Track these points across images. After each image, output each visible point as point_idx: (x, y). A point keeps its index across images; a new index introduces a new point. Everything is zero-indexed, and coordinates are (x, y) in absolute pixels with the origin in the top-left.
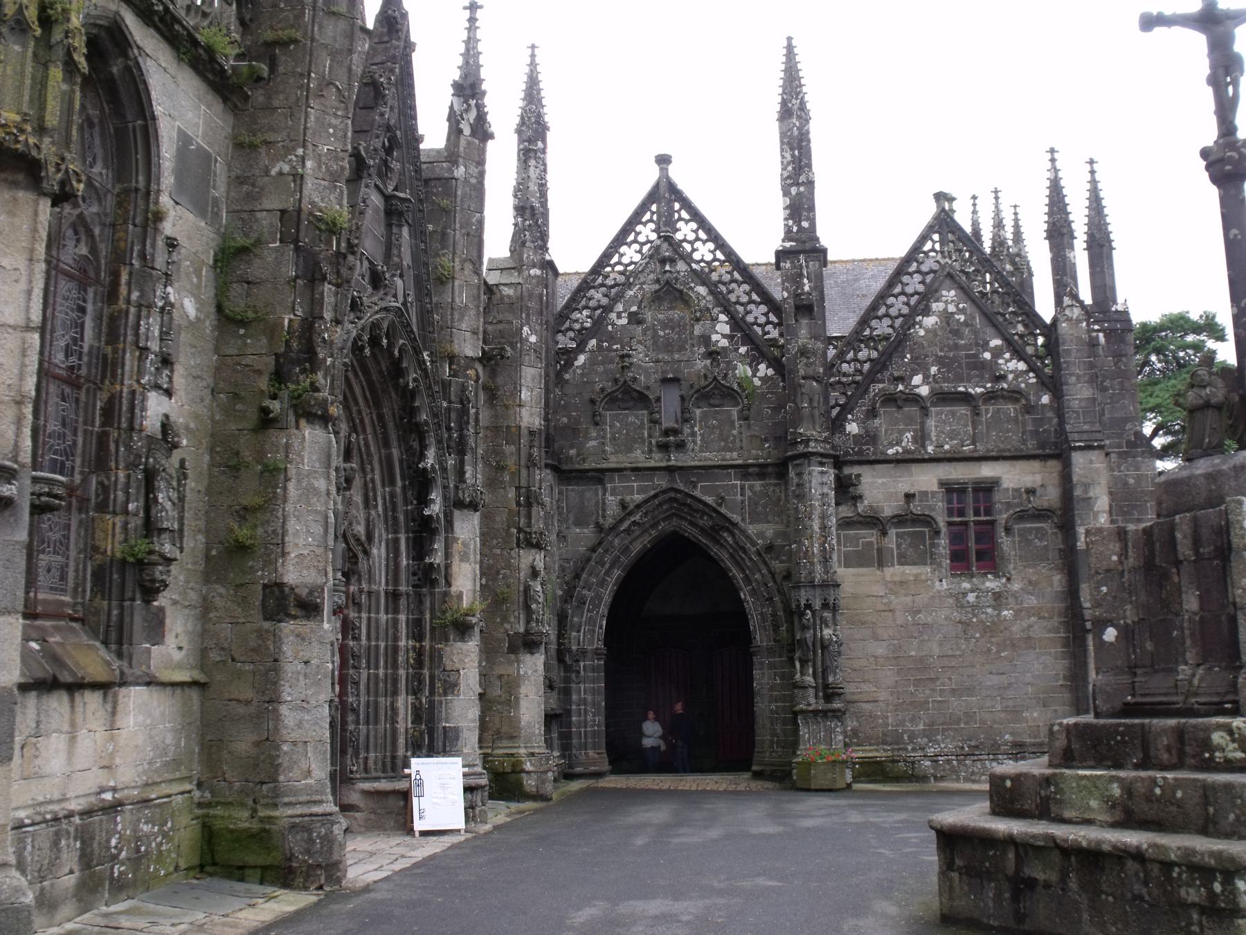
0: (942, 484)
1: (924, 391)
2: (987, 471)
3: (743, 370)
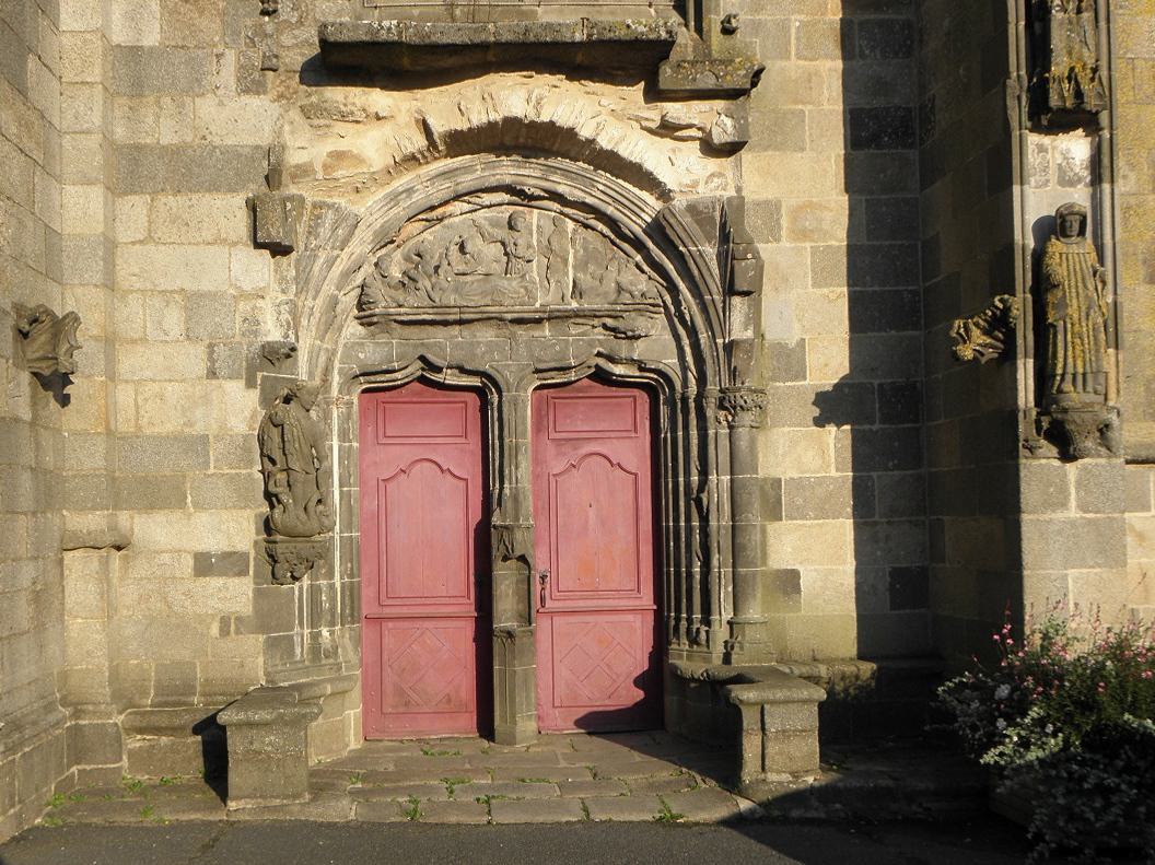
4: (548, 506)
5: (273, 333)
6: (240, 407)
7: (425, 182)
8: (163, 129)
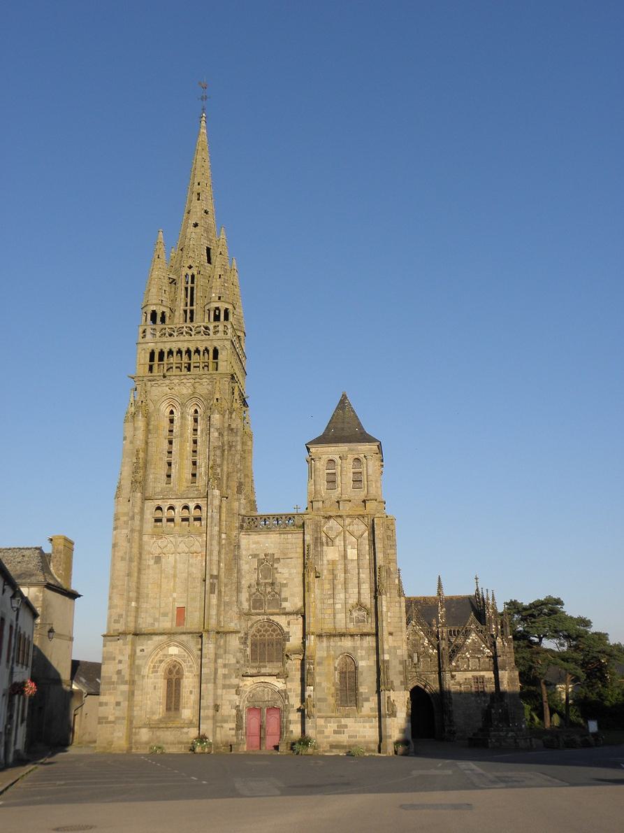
0: (473, 676)
1: (469, 656)
2: (482, 673)
3: (431, 651)
4: (267, 722)
5: (238, 704)
6: (234, 712)
7: (254, 686)
8: (228, 682)
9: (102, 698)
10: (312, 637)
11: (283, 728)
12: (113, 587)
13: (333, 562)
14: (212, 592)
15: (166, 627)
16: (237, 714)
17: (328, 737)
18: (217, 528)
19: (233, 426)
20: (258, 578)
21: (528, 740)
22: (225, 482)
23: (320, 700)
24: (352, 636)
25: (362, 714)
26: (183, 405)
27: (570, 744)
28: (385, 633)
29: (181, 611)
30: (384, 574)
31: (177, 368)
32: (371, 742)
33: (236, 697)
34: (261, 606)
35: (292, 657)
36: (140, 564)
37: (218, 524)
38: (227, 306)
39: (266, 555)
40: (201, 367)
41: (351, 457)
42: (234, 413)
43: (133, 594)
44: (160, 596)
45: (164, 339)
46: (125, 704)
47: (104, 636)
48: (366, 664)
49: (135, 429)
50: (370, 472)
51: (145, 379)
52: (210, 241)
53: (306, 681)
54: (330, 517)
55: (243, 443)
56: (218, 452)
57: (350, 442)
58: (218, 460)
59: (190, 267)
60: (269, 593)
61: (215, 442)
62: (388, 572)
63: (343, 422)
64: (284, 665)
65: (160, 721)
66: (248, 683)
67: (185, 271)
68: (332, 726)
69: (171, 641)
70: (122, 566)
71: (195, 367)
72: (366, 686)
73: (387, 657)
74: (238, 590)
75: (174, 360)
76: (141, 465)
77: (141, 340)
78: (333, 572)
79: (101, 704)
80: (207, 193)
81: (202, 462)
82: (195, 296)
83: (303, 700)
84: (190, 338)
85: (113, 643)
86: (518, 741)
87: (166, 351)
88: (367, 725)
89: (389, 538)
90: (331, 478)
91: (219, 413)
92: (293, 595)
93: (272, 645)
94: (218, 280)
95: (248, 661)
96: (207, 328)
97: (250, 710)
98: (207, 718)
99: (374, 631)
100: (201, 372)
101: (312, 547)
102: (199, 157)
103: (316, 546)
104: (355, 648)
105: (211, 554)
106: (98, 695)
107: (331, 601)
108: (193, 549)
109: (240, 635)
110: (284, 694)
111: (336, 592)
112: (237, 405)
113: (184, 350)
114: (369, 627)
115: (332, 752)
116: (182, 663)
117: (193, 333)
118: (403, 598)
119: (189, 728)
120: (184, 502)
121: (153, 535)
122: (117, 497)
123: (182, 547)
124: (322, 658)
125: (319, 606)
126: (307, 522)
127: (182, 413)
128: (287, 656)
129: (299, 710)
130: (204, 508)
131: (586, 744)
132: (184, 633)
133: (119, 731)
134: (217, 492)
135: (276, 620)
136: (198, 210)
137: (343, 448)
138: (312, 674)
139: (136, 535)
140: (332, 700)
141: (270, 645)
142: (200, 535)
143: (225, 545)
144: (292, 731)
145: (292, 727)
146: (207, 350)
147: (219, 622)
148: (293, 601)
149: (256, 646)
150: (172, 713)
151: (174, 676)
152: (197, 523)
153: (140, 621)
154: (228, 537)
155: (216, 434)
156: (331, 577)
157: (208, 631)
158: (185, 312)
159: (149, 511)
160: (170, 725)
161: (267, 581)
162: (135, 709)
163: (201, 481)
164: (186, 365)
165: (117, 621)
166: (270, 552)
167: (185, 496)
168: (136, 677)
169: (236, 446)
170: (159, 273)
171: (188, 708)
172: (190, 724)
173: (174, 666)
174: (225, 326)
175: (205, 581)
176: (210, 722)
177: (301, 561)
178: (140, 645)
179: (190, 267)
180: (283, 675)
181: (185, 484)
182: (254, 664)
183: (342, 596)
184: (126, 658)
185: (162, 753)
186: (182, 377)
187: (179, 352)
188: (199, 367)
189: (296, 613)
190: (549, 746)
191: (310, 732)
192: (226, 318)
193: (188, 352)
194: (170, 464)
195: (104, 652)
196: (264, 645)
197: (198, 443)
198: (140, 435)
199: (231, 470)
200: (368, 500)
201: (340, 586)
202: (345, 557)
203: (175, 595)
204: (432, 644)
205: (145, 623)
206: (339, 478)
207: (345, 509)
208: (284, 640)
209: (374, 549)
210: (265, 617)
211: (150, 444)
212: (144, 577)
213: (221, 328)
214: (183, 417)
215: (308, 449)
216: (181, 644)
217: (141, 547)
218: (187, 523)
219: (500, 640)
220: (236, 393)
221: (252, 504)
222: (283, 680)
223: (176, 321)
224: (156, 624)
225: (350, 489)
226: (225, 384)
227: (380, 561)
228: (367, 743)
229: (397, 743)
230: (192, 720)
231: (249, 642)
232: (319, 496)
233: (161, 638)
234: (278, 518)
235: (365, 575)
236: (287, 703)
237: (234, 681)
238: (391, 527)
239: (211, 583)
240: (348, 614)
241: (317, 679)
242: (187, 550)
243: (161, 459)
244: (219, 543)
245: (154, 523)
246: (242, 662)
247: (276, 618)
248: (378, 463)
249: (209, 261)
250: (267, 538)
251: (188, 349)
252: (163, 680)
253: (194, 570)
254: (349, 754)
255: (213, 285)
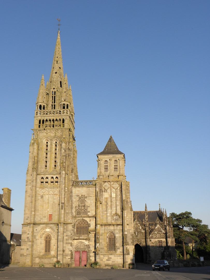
1: (156, 233)
2: (161, 239)
3: (142, 231)
6: (70, 252)
7: (77, 243)
9: (22, 247)
10: (99, 225)
11: (88, 258)
12: (26, 207)
13: (107, 198)
14: (62, 209)
15: (45, 221)
16: (71, 253)
17: (104, 262)
18: (64, 186)
19: (70, 148)
20: (79, 204)
21: (178, 264)
22: (67, 168)
23: (101, 248)
24: (113, 225)
25: (117, 253)
26: (51, 140)
27: (193, 265)
28: (126, 224)
29: (51, 216)
30: (125, 203)
31: (49, 126)
32: (120, 264)
33: (71, 247)
34: (80, 214)
35: (91, 233)
36: (35, 198)
37: (64, 184)
38: (68, 103)
39: (82, 195)
40: (58, 126)
41: (113, 160)
42: (70, 143)
43: (33, 209)
44: (43, 210)
45: (44, 115)
46: (30, 249)
47: (22, 225)
48: (118, 235)
49: (34, 149)
50: (121, 165)
51: (37, 130)
52: (61, 79)
53: (96, 241)
54: (105, 182)
55: (74, 154)
56: (64, 158)
57: (113, 154)
58: (64, 161)
59: (54, 89)
60: (83, 209)
61: (63, 154)
62: (127, 202)
63: (111, 147)
64: (88, 236)
65: (43, 255)
66: (75, 242)
67: (52, 90)
68: (106, 258)
69: (47, 226)
70: (29, 199)
71: (56, 126)
72: (119, 243)
73: (126, 233)
74: (72, 208)
75: (48, 123)
76: (36, 162)
77: (36, 116)
78: (106, 202)
79: (21, 249)
80: (60, 61)
81: (58, 161)
82: (56, 99)
83: (95, 248)
84: (54, 115)
85: (26, 227)
86: (174, 264)
87: (45, 120)
88: (119, 258)
89: (127, 189)
90: (106, 167)
91: (65, 143)
92: (91, 210)
93: (84, 228)
94: (64, 93)
95: (75, 234)
96: (60, 111)
97: (76, 252)
98: (60, 254)
99: (122, 224)
100: (58, 128)
101: (99, 192)
102: (57, 47)
103: (100, 192)
104: (114, 230)
105: (62, 195)
106: (20, 246)
107: (106, 213)
108: (55, 193)
109: (72, 225)
110: (88, 246)
111: (108, 209)
112: (71, 140)
113: (52, 120)
114: (120, 222)
115: (106, 267)
116: (51, 235)
117: (55, 113)
118: (132, 212)
119: (53, 258)
120: (52, 176)
121: (40, 188)
122: (27, 174)
123: (51, 192)
124: (103, 233)
125: (101, 214)
126: (97, 183)
127: (51, 143)
128: (89, 232)
129: (94, 252)
130: (59, 178)
131: (199, 266)
132: (52, 224)
133: (28, 259)
134: (64, 172)
135: (85, 219)
136: (57, 67)
137: (111, 156)
138: (99, 239)
139: (34, 188)
140: (106, 249)
141: (83, 228)
142: (58, 188)
143: (67, 191)
144: (91, 260)
145: (91, 258)
146: (60, 119)
147: (64, 220)
148: (92, 212)
149: (78, 228)
150: (47, 253)
151: (48, 239)
152: (56, 183)
153: (36, 219)
154: (68, 189)
155: (64, 151)
156: (106, 204)
157: (60, 223)
158: (52, 105)
159: (38, 179)
160: (47, 257)
161: (82, 205)
162: (34, 251)
163: (58, 168)
164: (52, 125)
165: (27, 219)
166: (83, 194)
167: (52, 174)
168: (34, 240)
169: (71, 155)
170: (43, 91)
171: (53, 251)
172: (54, 257)
173: (48, 236)
174: (67, 111)
175: (59, 205)
176: (61, 256)
177: (95, 198)
178: (35, 228)
179: (54, 89)
180: (88, 239)
181: (52, 169)
182: (77, 235)
183: (110, 211)
184: (30, 233)
185: (44, 267)
186: (51, 130)
187: (50, 120)
188: (57, 126)
189: (93, 217)
190: (186, 266)
191: (98, 260)
192: (67, 108)
193: (53, 120)
194: (46, 162)
195: (22, 230)
196: (81, 228)
197: (57, 154)
198: (36, 151)
199: (69, 164)
200: (120, 176)
201: (109, 207)
202: (111, 196)
203: (48, 210)
204: (143, 228)
205: (37, 220)
206: (109, 167)
207: (111, 179)
208: (88, 227)
209: (122, 193)
210: (82, 218)
211: (39, 154)
212: (37, 203)
213: (65, 111)
214: (51, 145)
215: (98, 156)
216: (51, 228)
217: (36, 192)
218: (53, 183)
219: (168, 227)
220: (71, 135)
221: (77, 177)
222: (88, 241)
223: (49, 109)
224: (42, 220)
225: (113, 172)
226: (67, 132)
227: (124, 198)
228: (118, 264)
229: (130, 264)
230: (55, 255)
231: (75, 227)
232: (101, 174)
233: (43, 225)
234: (86, 182)
235: (119, 203)
236: (89, 249)
237: (70, 241)
238: (128, 185)
239: (62, 206)
240: (112, 217)
241: (101, 241)
242: (53, 193)
243: (43, 160)
244: (65, 191)
245: (40, 184)
246: (73, 234)
247: (85, 219)
248: (124, 162)
249: (61, 86)
250: (82, 189)
251: (53, 119)
252: (44, 241)
253: (55, 201)
254: (112, 268)
255: (63, 95)
